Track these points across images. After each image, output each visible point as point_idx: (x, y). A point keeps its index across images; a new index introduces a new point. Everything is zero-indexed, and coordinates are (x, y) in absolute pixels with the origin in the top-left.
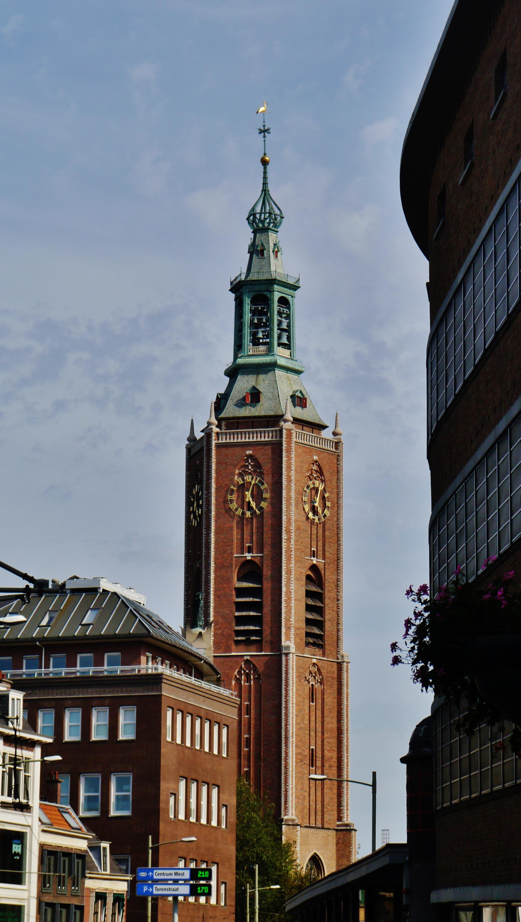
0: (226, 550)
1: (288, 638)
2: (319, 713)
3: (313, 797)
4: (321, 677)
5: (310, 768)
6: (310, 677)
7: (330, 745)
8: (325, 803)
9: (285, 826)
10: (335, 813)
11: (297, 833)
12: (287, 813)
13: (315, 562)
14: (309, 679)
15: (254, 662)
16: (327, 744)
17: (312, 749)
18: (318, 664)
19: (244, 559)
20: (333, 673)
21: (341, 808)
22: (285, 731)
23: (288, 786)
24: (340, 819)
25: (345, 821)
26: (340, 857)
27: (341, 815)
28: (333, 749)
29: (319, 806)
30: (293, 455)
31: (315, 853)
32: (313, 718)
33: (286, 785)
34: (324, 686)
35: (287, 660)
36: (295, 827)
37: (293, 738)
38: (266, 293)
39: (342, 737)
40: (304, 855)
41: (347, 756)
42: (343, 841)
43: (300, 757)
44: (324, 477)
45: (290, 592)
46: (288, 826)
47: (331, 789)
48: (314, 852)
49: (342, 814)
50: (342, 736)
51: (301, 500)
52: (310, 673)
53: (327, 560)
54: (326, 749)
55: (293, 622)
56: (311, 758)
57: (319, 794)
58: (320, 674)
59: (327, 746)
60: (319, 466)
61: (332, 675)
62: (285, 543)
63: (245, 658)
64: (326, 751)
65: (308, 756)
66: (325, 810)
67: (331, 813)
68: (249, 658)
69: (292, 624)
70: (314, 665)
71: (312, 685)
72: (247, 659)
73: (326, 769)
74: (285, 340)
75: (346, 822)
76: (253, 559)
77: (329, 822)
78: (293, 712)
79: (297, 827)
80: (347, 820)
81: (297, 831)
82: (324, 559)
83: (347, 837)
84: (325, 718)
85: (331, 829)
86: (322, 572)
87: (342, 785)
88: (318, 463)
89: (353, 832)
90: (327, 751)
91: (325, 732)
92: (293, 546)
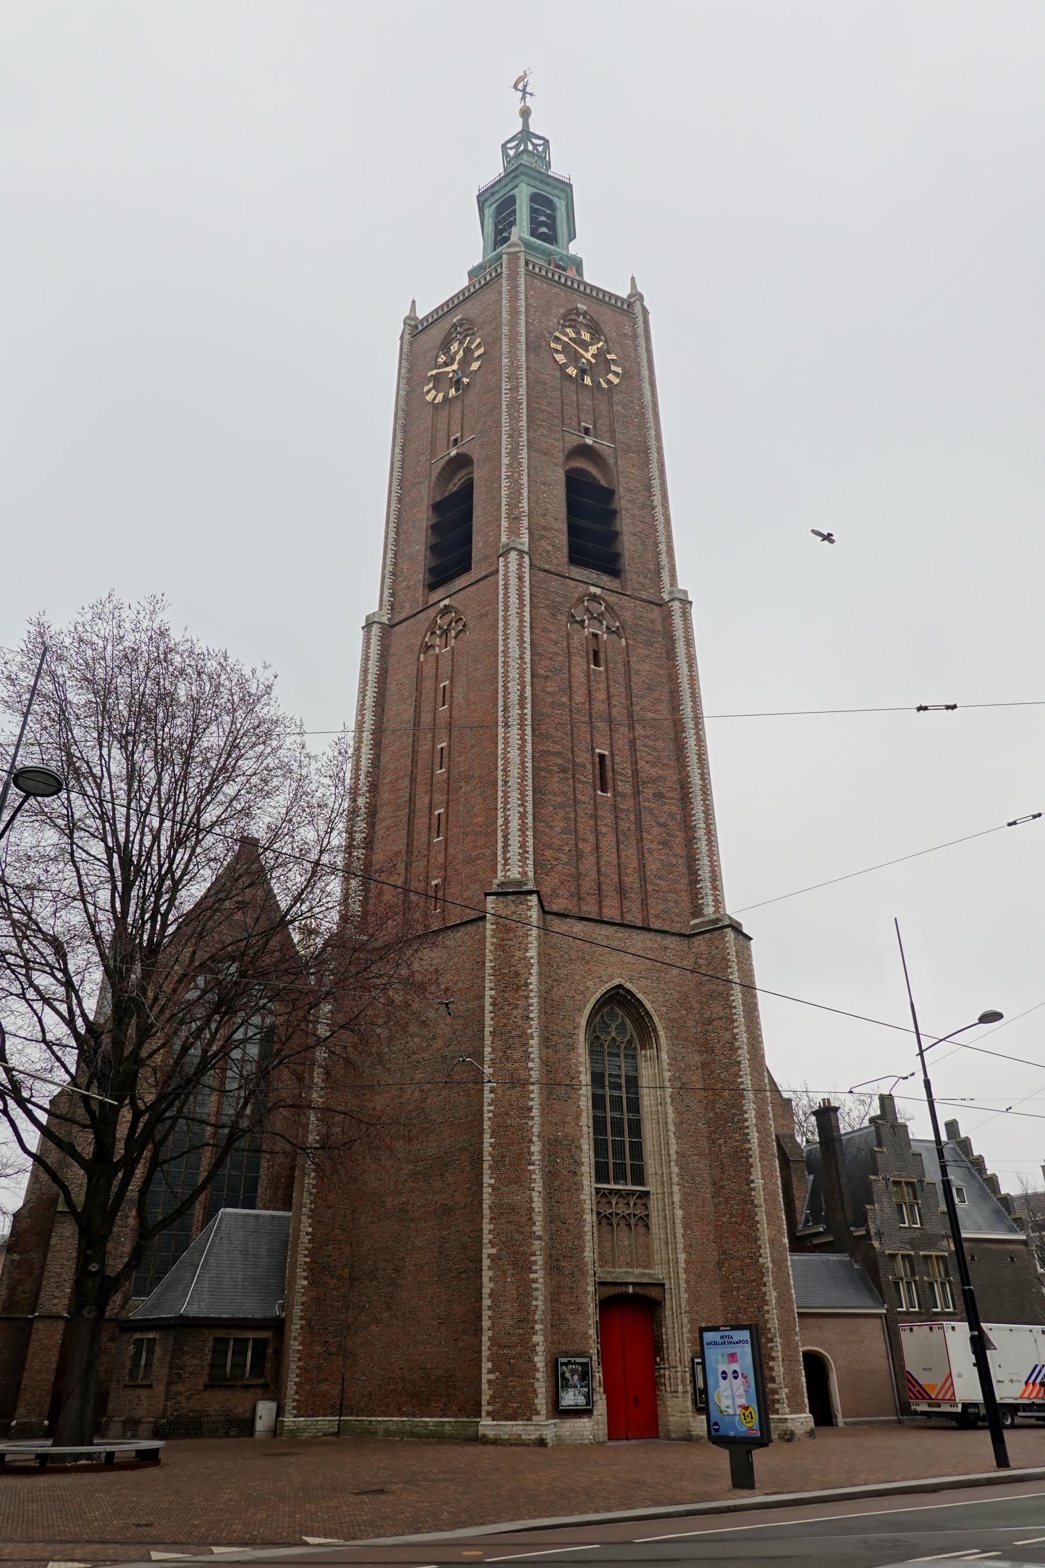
0: (420, 461)
1: (514, 531)
2: (618, 690)
3: (609, 856)
4: (618, 624)
5: (595, 791)
6: (586, 617)
7: (656, 754)
8: (648, 873)
9: (494, 897)
10: (685, 897)
11: (529, 913)
12: (508, 874)
13: (589, 441)
14: (583, 621)
15: (456, 605)
16: (642, 748)
17: (602, 757)
18: (606, 597)
19: (447, 458)
20: (653, 621)
21: (698, 886)
22: (504, 697)
23: (509, 810)
24: (697, 911)
25: (709, 910)
26: (704, 1000)
27: (700, 902)
28: (665, 762)
29: (631, 880)
30: (522, 281)
31: (620, 986)
32: (600, 695)
33: (505, 809)
34: (626, 639)
35: (506, 566)
36: (522, 897)
37: (522, 707)
38: (511, 193)
39: (686, 738)
40: (582, 988)
41: (702, 774)
42: (706, 959)
43: (559, 761)
44: (604, 336)
45: (520, 464)
46: (501, 899)
47: (665, 843)
48: (617, 982)
49: (702, 898)
50: (684, 735)
51: (547, 348)
52: (588, 610)
53: (617, 444)
54: (642, 759)
55: (526, 508)
56: (597, 772)
57: (630, 852)
58: (616, 617)
59: (644, 754)
60: (592, 320)
61: (650, 625)
62: (506, 394)
63: (442, 604)
64: (641, 763)
65: (589, 767)
66: (650, 888)
67: (671, 896)
68: (447, 602)
69: (524, 512)
70: (594, 598)
71: (595, 635)
72: (445, 606)
73: (647, 800)
74: (544, 230)
75: (714, 917)
76: (460, 450)
77: (665, 916)
78: (521, 658)
79: (529, 898)
80: (715, 912)
81: (529, 908)
82: (613, 440)
83: (717, 948)
84: (634, 699)
85: (674, 934)
86: (611, 461)
87: (696, 835)
88: (590, 315)
89: (730, 934)
90: (647, 762)
91: (636, 725)
92: (524, 397)
